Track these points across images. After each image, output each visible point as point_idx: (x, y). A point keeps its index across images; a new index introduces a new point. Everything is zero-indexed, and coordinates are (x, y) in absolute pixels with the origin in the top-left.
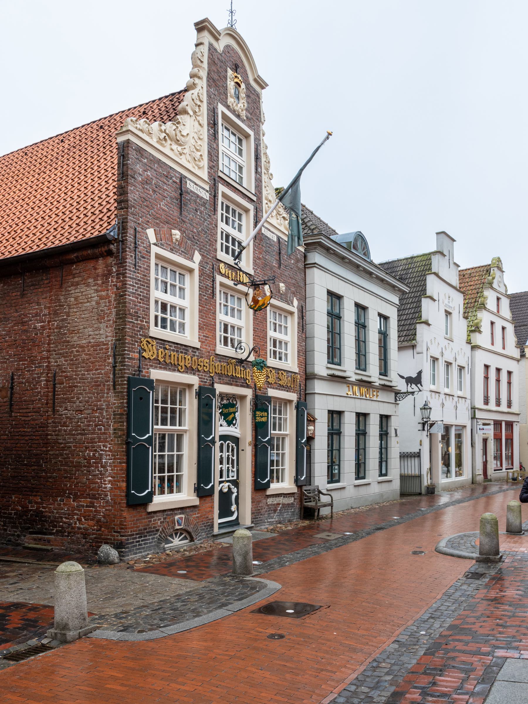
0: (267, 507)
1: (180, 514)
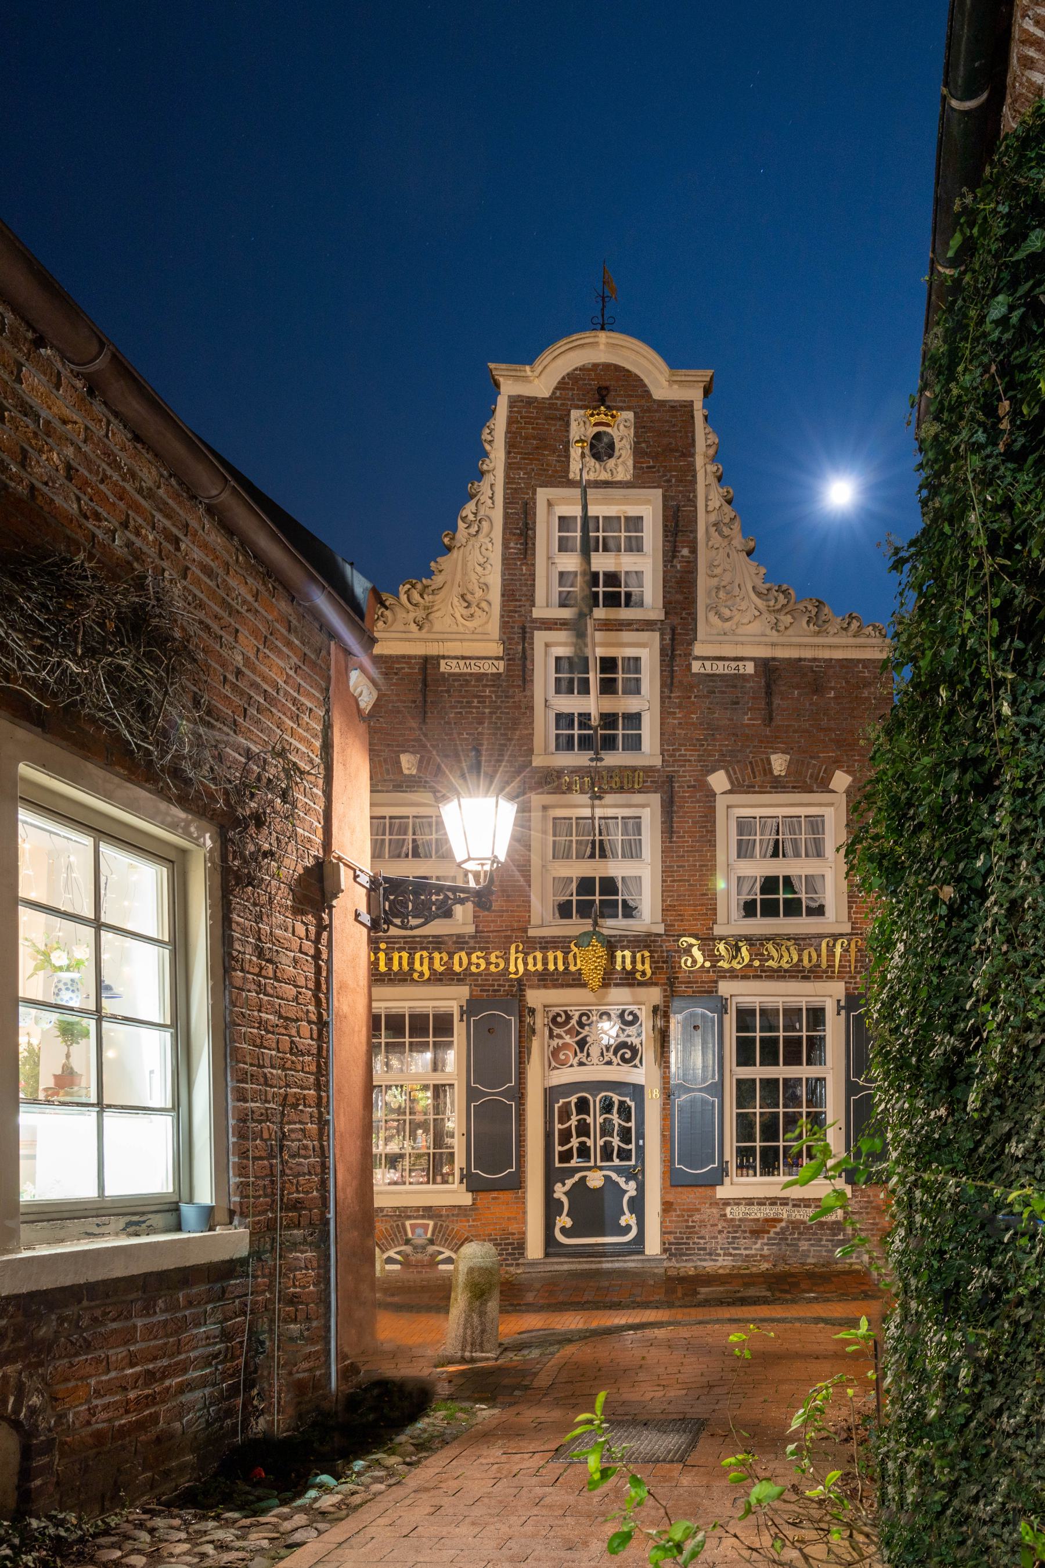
1: (423, 1217)
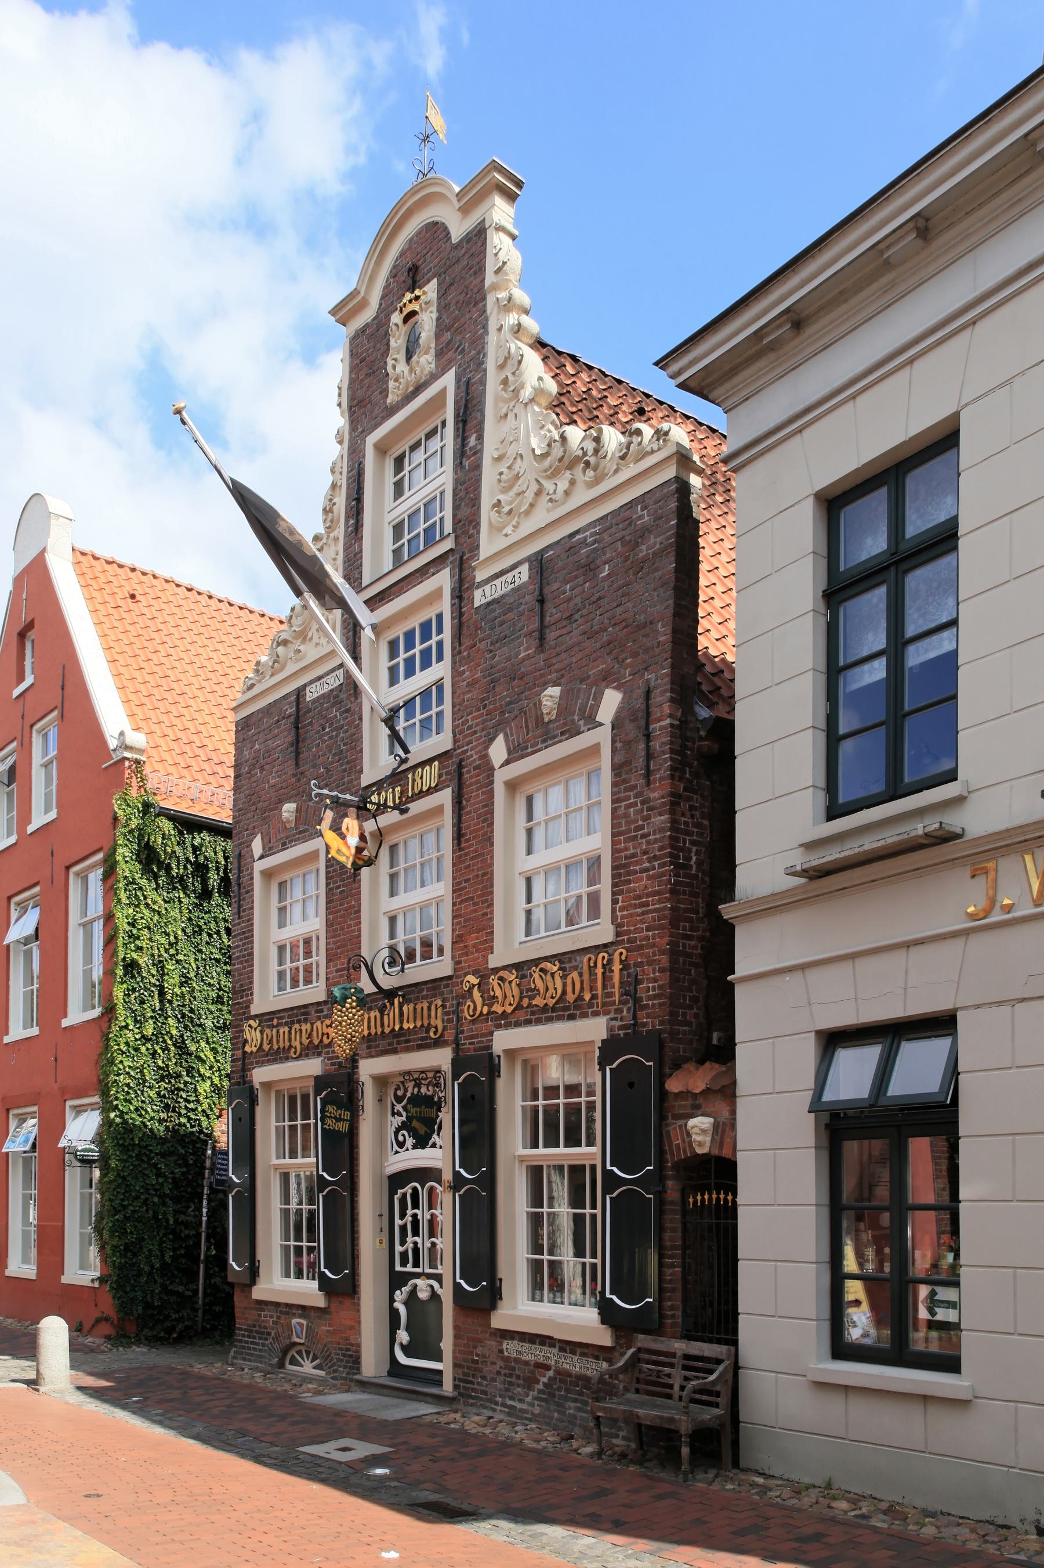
0: (500, 1363)
1: (301, 1316)
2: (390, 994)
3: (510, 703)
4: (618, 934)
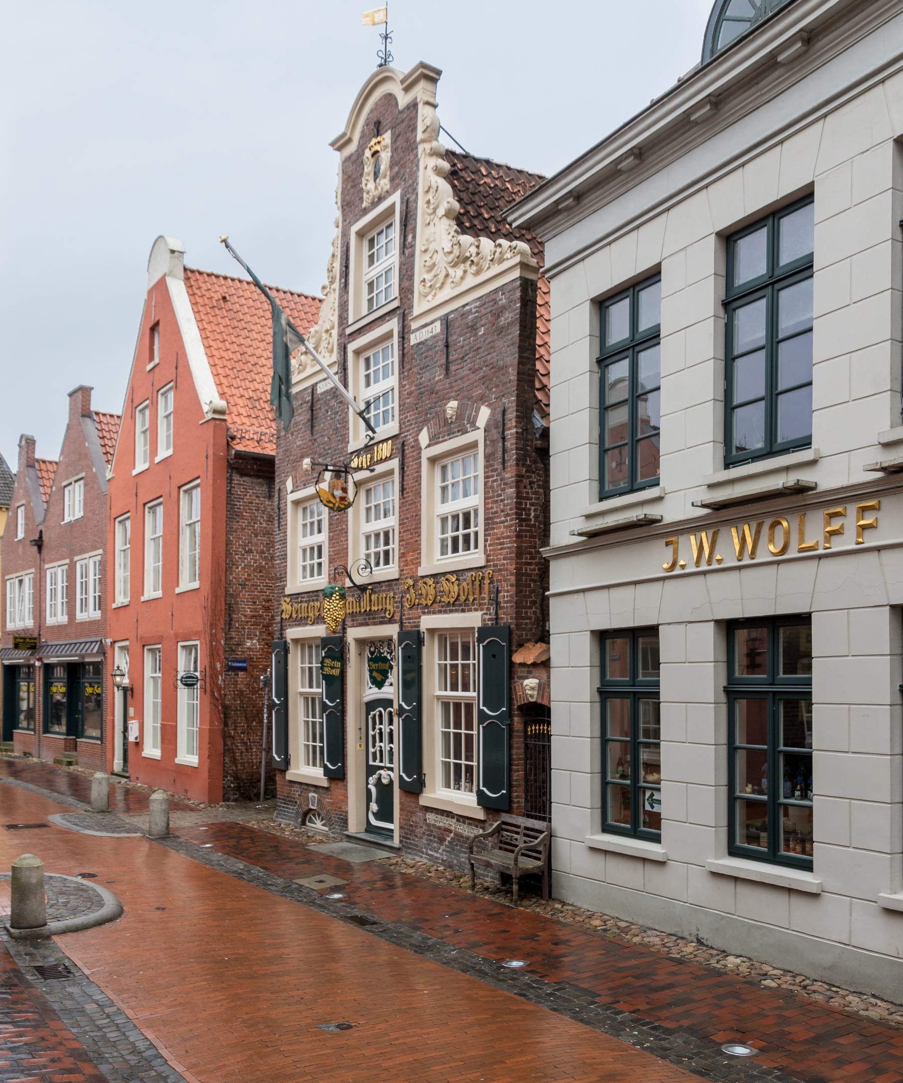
0: (425, 827)
1: (314, 792)
2: (363, 588)
3: (430, 408)
4: (488, 561)
